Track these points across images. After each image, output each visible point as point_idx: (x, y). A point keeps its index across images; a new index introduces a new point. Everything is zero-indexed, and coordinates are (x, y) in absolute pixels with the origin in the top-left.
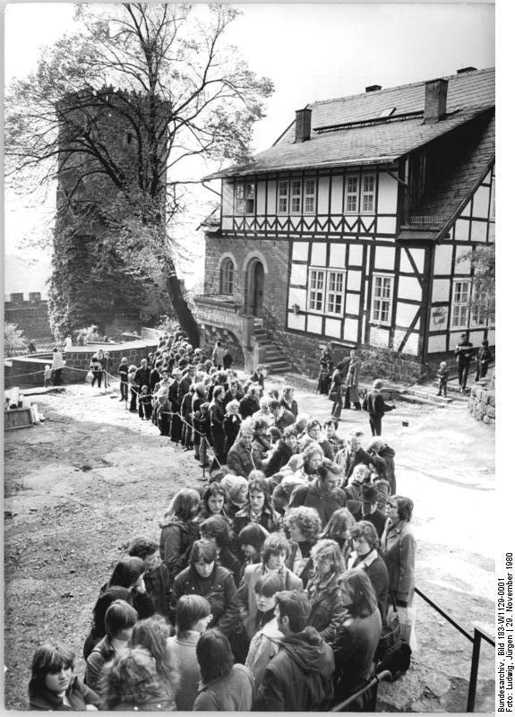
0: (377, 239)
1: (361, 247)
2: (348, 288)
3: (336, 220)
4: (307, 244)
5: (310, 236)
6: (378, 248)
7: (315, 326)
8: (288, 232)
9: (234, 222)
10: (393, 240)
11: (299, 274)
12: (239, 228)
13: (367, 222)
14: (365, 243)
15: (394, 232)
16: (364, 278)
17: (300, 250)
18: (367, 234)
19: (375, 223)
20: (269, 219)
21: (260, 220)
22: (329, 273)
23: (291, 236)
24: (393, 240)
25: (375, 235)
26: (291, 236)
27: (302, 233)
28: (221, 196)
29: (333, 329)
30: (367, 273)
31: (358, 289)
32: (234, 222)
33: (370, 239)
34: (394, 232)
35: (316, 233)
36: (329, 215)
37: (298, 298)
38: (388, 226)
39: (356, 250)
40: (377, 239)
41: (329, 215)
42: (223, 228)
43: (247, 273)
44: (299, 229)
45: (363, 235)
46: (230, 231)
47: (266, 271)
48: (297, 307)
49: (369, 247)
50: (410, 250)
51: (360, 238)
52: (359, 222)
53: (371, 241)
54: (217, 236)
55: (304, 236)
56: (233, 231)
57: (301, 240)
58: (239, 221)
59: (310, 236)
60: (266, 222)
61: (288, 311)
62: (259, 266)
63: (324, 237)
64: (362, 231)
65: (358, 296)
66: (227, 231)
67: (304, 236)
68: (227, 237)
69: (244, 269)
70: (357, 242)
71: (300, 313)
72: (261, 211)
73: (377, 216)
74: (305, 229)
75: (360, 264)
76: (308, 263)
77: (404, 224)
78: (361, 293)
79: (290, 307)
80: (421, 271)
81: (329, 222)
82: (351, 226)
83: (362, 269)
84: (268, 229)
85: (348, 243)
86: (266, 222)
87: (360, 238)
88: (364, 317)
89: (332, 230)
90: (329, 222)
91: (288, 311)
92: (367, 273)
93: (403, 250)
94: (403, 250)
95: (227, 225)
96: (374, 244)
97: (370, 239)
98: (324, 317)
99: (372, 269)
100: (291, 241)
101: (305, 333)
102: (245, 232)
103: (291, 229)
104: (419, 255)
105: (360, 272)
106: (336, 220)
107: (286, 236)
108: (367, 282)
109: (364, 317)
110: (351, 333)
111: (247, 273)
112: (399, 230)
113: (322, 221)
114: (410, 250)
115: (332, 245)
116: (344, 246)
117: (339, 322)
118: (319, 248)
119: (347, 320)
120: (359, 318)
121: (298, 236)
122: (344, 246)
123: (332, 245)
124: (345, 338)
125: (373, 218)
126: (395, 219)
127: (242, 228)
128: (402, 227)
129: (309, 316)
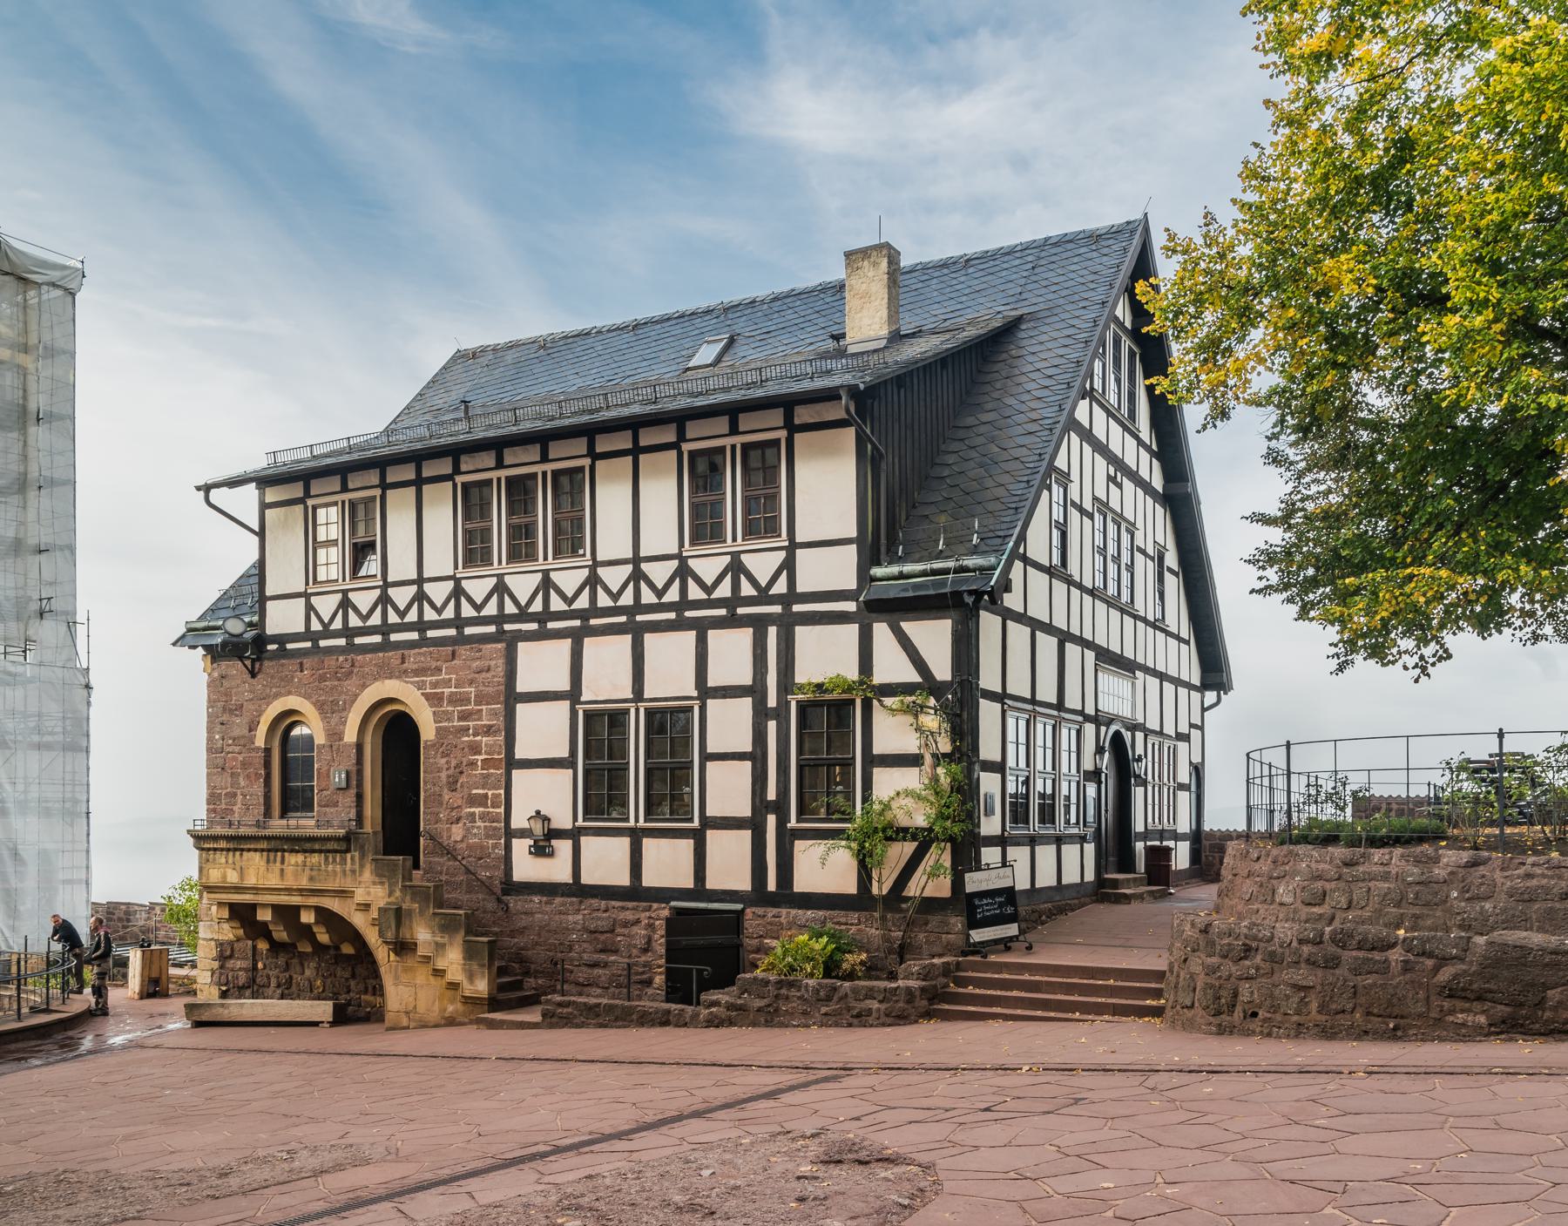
0: (796, 608)
1: (745, 635)
4: (566, 644)
5: (577, 623)
6: (800, 632)
7: (605, 861)
8: (500, 618)
9: (310, 608)
10: (850, 606)
12: (326, 626)
13: (763, 564)
14: (759, 625)
15: (852, 584)
16: (761, 714)
17: (541, 665)
18: (763, 596)
19: (789, 566)
20: (427, 587)
21: (402, 596)
22: (642, 711)
23: (507, 627)
24: (850, 606)
25: (792, 596)
26: (507, 627)
27: (547, 615)
28: (261, 534)
29: (667, 863)
30: (772, 702)
32: (310, 608)
33: (777, 609)
34: (852, 584)
35: (595, 611)
36: (636, 560)
38: (831, 570)
39: (732, 655)
40: (796, 608)
41: (636, 560)
42: (269, 631)
43: (359, 747)
44: (537, 606)
45: (750, 601)
46: (296, 637)
49: (772, 631)
50: (904, 625)
51: (740, 611)
53: (781, 616)
54: (239, 645)
55: (551, 625)
56: (308, 635)
57: (542, 635)
59: (577, 623)
60: (421, 597)
61: (510, 834)
63: (623, 619)
64: (747, 590)
66: (281, 639)
67: (551, 625)
68: (283, 653)
69: (350, 736)
70: (732, 622)
74: (557, 604)
75: (747, 680)
76: (573, 694)
77: (879, 564)
79: (519, 821)
80: (942, 670)
81: (637, 576)
83: (755, 691)
84: (430, 614)
85: (702, 628)
86: (421, 597)
88: (771, 820)
89: (648, 597)
90: (637, 576)
91: (510, 834)
92: (772, 702)
93: (881, 631)
94: (881, 631)
95: (283, 618)
96: (788, 625)
97: (777, 609)
98: (636, 836)
99: (786, 682)
100: (512, 641)
101: (577, 890)
102: (348, 632)
103: (510, 608)
104: (934, 638)
105: (746, 703)
106: (659, 573)
107: (492, 629)
108: (772, 726)
109: (771, 820)
110: (730, 861)
112: (864, 577)
113: (614, 577)
114: (907, 626)
115: (649, 639)
116: (690, 637)
117: (687, 845)
119: (711, 835)
120: (755, 824)
121: (534, 626)
122: (690, 637)
123: (649, 639)
124: (712, 883)
125: (783, 554)
126: (852, 549)
127: (337, 624)
128: (877, 571)
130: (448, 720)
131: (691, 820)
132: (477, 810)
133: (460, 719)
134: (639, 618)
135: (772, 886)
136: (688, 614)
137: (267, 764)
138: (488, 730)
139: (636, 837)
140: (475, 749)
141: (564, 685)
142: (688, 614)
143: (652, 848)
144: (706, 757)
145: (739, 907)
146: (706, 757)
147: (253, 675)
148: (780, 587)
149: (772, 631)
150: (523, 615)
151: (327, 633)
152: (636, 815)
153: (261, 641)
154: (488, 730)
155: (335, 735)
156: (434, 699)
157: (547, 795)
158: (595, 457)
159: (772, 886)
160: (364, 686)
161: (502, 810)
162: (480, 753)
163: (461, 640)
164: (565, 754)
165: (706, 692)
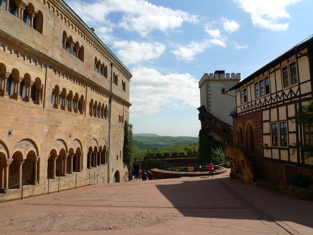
2: (289, 131)
3: (280, 94)
4: (268, 111)
7: (275, 154)
8: (261, 107)
9: (241, 108)
11: (266, 128)
13: (295, 89)
14: (295, 102)
17: (266, 115)
19: (299, 89)
23: (262, 108)
25: (301, 95)
26: (262, 108)
29: (284, 155)
31: (294, 130)
32: (241, 108)
33: (298, 99)
35: (272, 104)
37: (267, 140)
45: (294, 98)
47: (253, 129)
48: (266, 145)
49: (298, 104)
51: (293, 100)
52: (291, 91)
56: (241, 113)
58: (242, 107)
59: (270, 106)
62: (251, 127)
63: (276, 105)
65: (295, 134)
69: (246, 130)
70: (291, 103)
71: (268, 148)
72: (249, 101)
73: (300, 84)
76: (269, 121)
78: (296, 132)
81: (277, 96)
82: (287, 95)
87: (293, 100)
96: (300, 101)
97: (298, 99)
106: (280, 94)
111: (247, 131)
113: (274, 96)
117: (287, 151)
118: (274, 112)
121: (264, 108)
122: (285, 107)
125: (298, 86)
129: (273, 150)
130: (256, 126)
131: (287, 146)
132: (260, 143)
133: (257, 126)
134: (278, 104)
135: (301, 162)
136: (285, 102)
137: (239, 135)
138: (260, 128)
139: (280, 149)
140: (259, 131)
141: (268, 119)
142: (285, 102)
143: (282, 151)
144: (289, 133)
145: (295, 166)
146: (289, 133)
147: (236, 120)
148: (298, 94)
149: (298, 104)
150: (263, 106)
151: (243, 112)
152: (279, 146)
153: (237, 114)
154: (260, 128)
155: (244, 129)
156: (254, 122)
157: (267, 140)
158: (270, 73)
159: (301, 162)
160: (246, 121)
161: (262, 143)
162: (259, 132)
163: (257, 111)
164: (269, 132)
165: (288, 119)
